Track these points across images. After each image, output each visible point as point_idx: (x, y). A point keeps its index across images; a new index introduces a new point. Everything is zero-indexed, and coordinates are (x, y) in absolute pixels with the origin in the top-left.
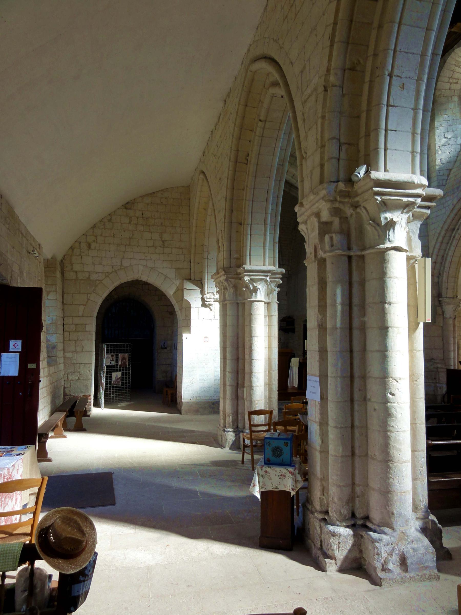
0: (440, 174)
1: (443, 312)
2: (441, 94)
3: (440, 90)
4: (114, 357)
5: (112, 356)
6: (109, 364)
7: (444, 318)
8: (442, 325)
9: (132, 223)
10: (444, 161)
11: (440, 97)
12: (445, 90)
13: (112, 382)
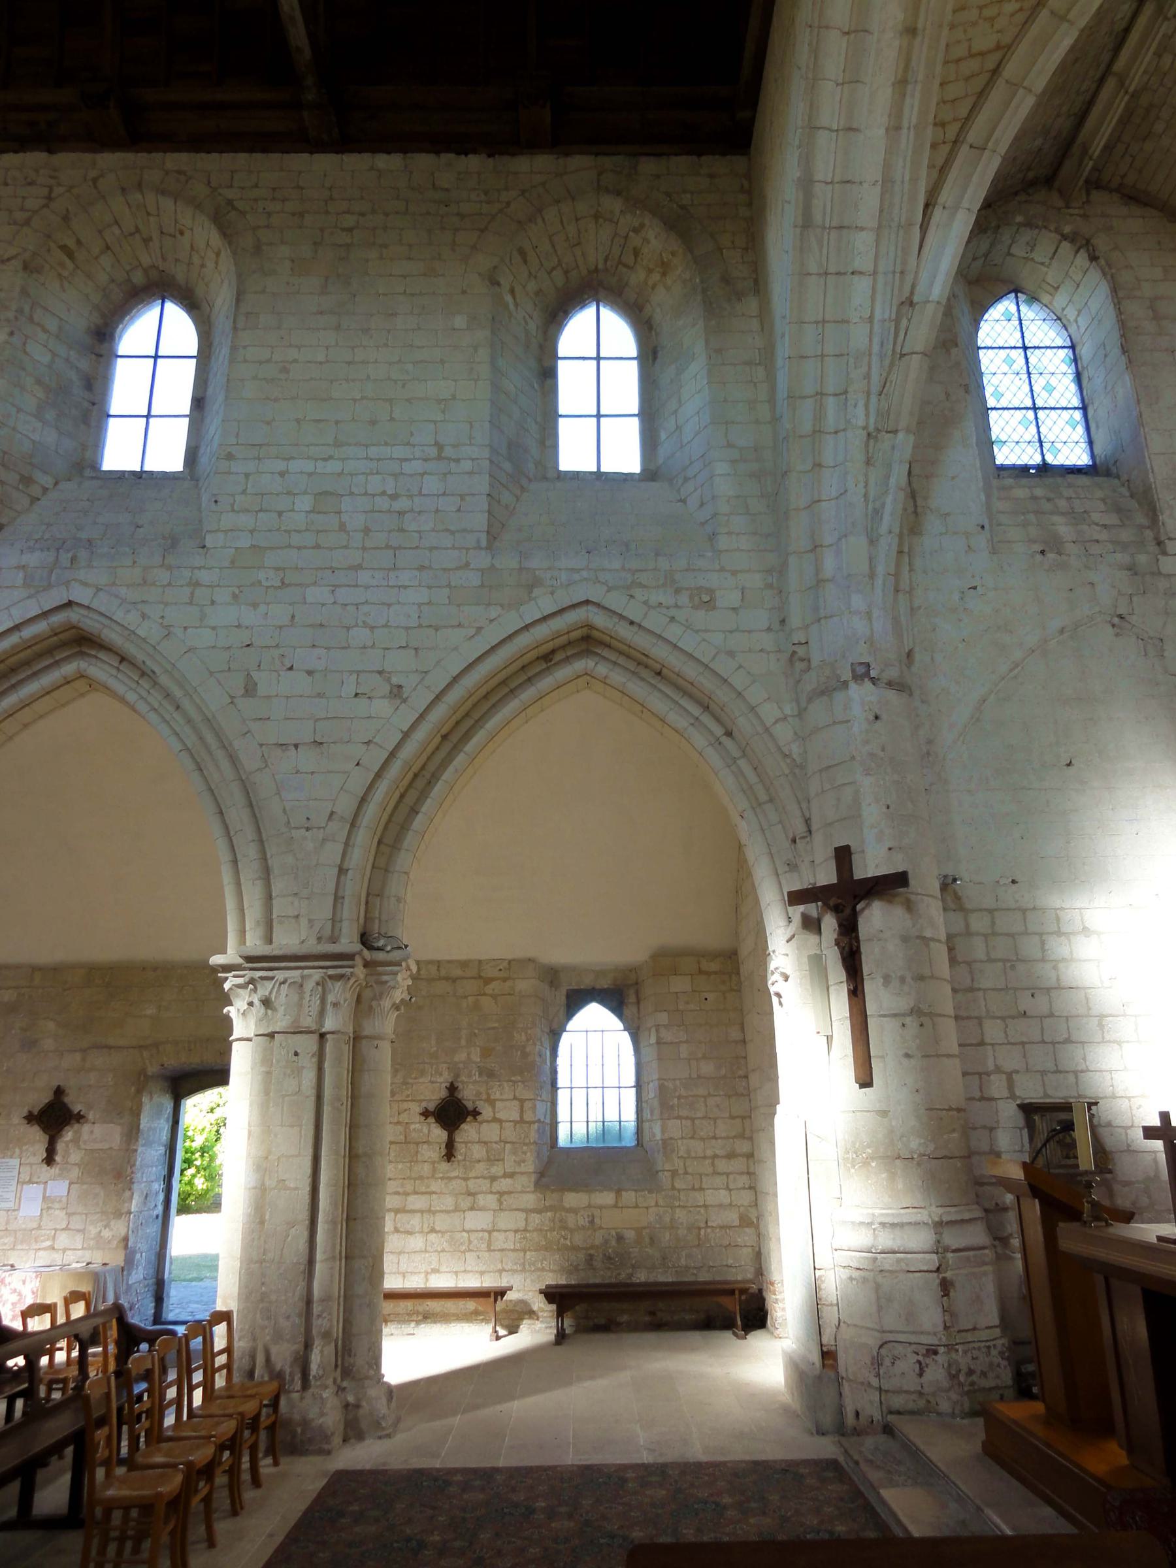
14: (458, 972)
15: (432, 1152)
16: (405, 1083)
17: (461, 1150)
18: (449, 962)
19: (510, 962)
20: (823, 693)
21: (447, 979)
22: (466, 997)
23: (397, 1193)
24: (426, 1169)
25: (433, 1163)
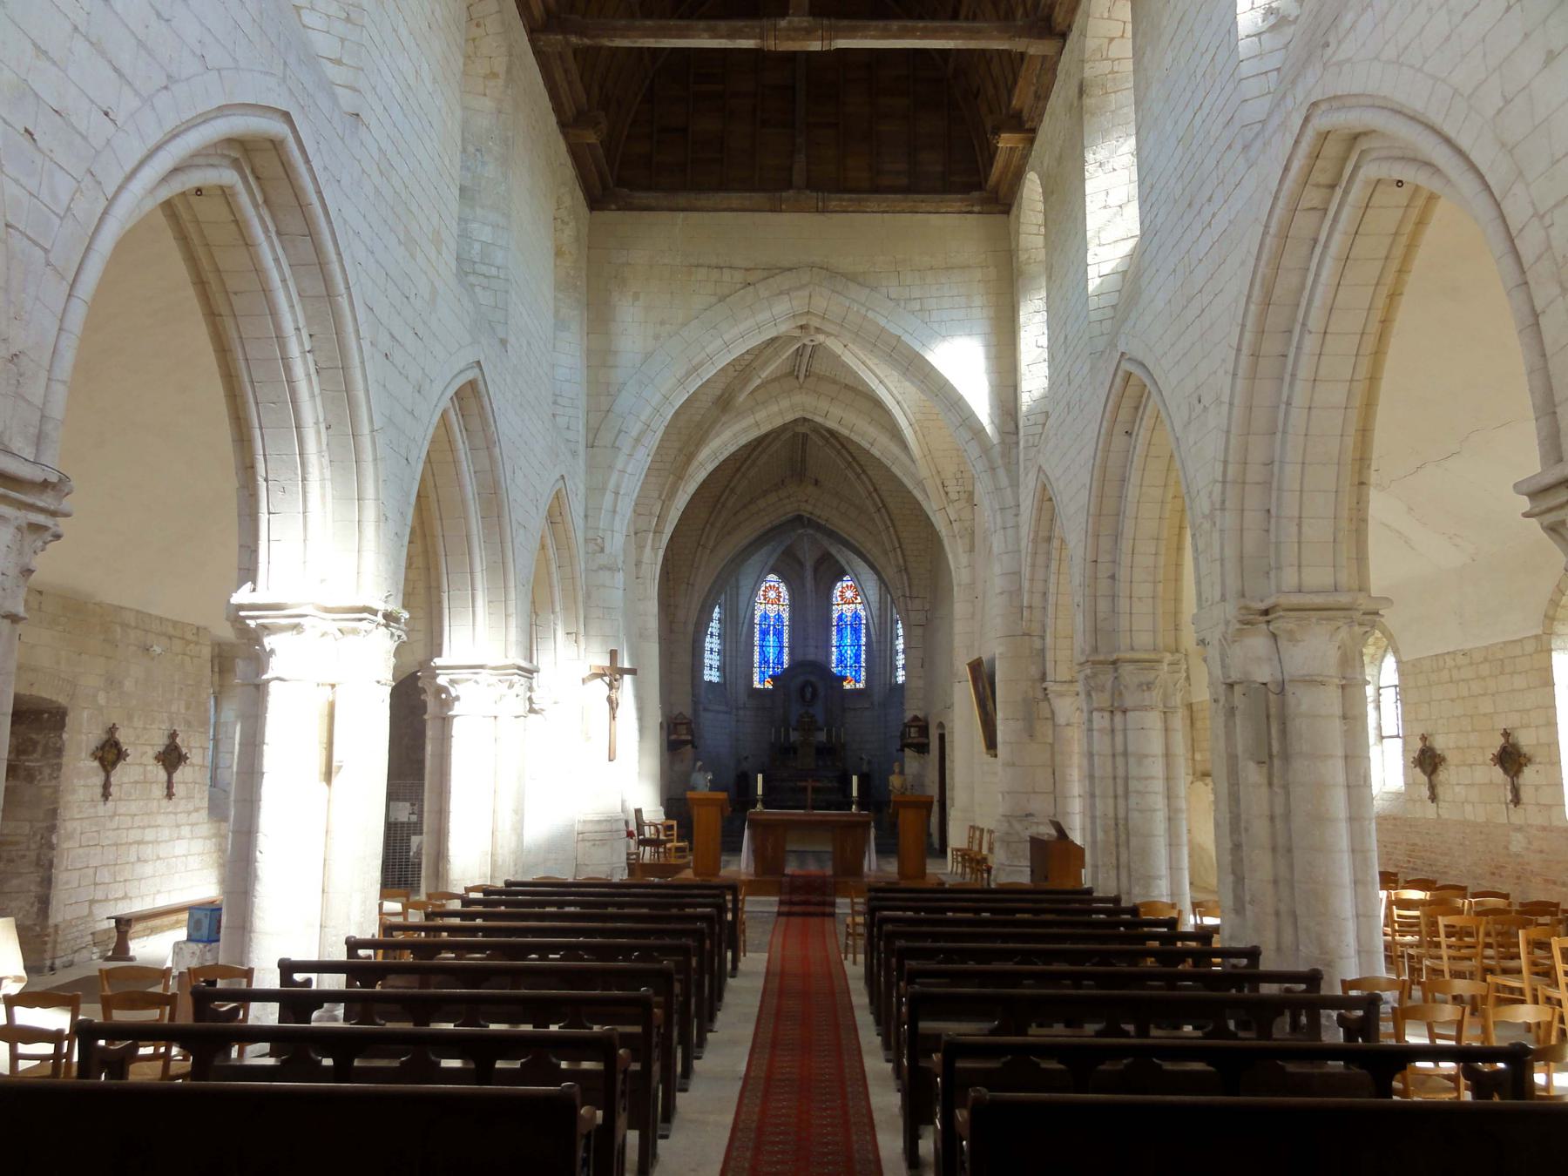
0: (1030, 423)
1: (1053, 712)
2: (1029, 258)
3: (1027, 250)
4: (416, 807)
5: (412, 805)
6: (406, 820)
7: (1054, 725)
8: (1050, 741)
9: (414, 566)
10: (1036, 394)
11: (1030, 264)
12: (1036, 249)
13: (411, 854)
14: (171, 631)
15: (159, 791)
16: (145, 729)
17: (179, 789)
18: (167, 620)
19: (198, 628)
20: (610, 569)
21: (164, 634)
22: (177, 654)
23: (139, 827)
24: (155, 803)
25: (159, 800)
